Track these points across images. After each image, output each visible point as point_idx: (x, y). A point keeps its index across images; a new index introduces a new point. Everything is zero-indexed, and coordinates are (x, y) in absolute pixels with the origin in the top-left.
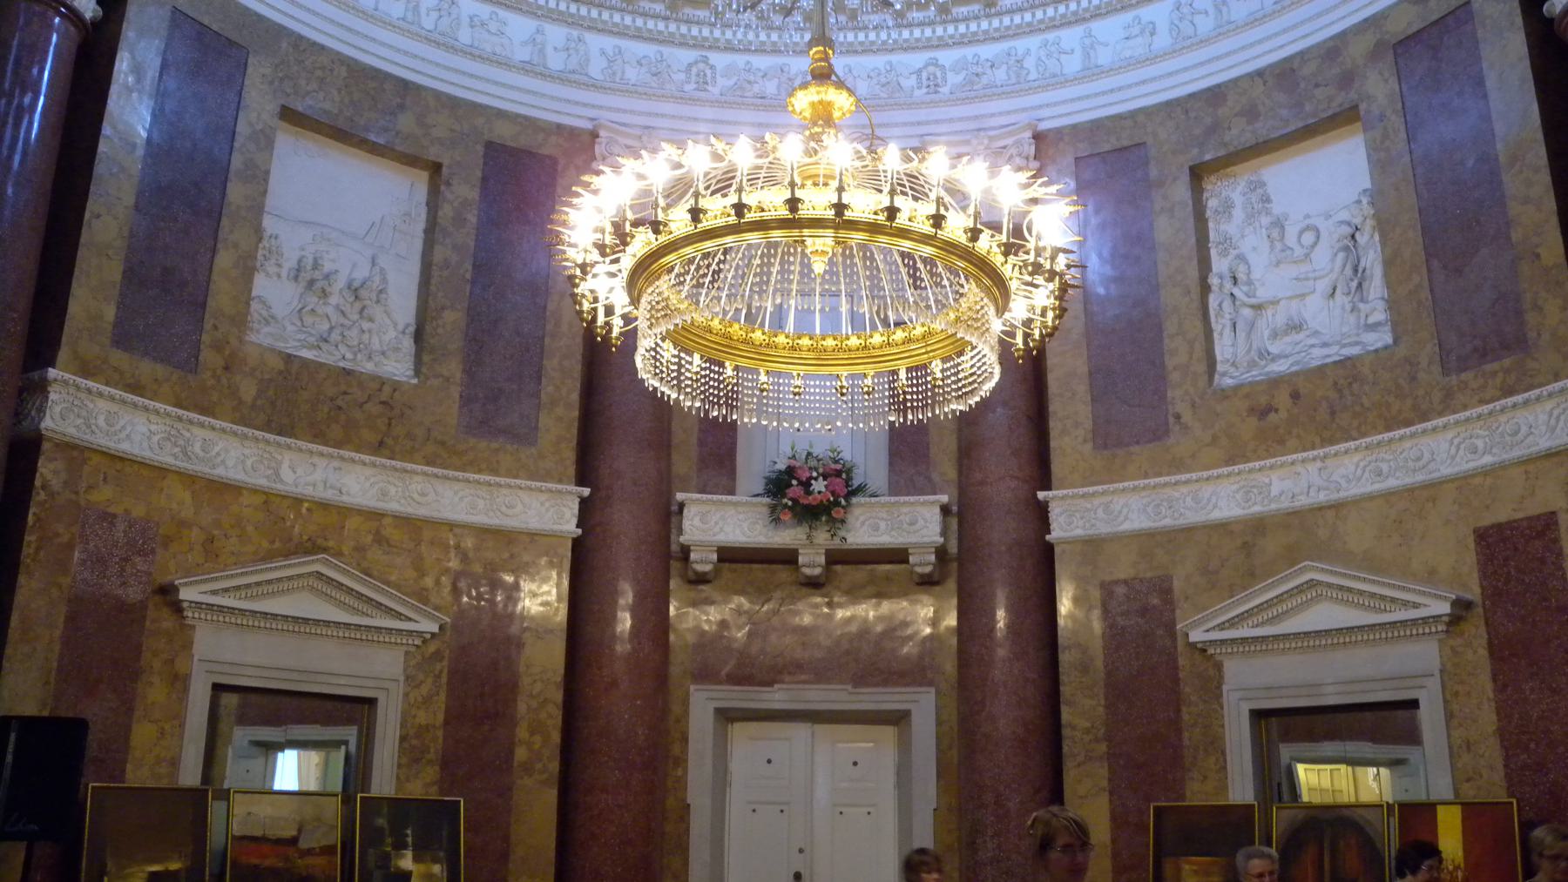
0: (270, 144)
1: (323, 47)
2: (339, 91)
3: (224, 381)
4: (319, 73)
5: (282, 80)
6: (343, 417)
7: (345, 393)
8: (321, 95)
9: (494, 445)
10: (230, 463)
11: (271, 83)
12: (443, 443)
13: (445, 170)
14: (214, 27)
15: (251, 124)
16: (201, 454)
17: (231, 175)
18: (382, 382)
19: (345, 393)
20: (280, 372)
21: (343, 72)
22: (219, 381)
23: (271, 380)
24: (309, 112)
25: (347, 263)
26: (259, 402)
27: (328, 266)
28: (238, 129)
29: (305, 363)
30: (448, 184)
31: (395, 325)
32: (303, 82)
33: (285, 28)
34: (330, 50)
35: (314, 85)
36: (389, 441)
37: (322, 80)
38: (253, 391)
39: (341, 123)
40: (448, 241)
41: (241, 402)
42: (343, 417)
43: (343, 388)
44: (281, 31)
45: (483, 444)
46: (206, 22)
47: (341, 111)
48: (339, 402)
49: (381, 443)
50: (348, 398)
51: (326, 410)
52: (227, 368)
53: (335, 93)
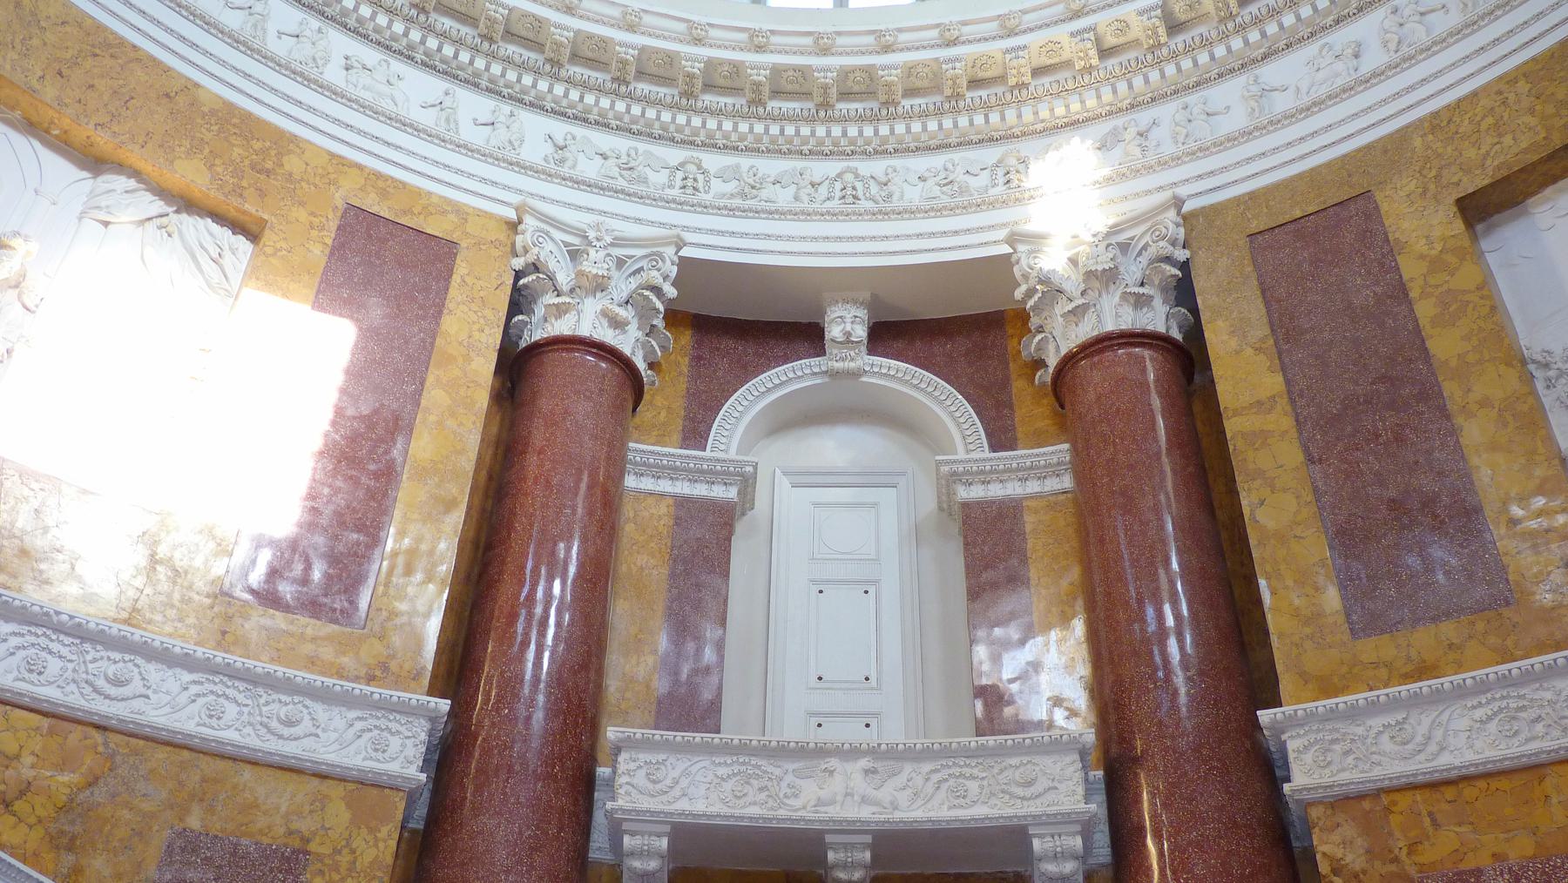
1: (1475, 94)
2: (1532, 111)
5: (1438, 177)
8: (1508, 140)
14: (1311, 209)
15: (1422, 257)
21: (1523, 86)
24: (1504, 172)
28: (1406, 277)
32: (1471, 153)
33: (1407, 127)
34: (1485, 88)
44: (1402, 135)
46: (1298, 214)
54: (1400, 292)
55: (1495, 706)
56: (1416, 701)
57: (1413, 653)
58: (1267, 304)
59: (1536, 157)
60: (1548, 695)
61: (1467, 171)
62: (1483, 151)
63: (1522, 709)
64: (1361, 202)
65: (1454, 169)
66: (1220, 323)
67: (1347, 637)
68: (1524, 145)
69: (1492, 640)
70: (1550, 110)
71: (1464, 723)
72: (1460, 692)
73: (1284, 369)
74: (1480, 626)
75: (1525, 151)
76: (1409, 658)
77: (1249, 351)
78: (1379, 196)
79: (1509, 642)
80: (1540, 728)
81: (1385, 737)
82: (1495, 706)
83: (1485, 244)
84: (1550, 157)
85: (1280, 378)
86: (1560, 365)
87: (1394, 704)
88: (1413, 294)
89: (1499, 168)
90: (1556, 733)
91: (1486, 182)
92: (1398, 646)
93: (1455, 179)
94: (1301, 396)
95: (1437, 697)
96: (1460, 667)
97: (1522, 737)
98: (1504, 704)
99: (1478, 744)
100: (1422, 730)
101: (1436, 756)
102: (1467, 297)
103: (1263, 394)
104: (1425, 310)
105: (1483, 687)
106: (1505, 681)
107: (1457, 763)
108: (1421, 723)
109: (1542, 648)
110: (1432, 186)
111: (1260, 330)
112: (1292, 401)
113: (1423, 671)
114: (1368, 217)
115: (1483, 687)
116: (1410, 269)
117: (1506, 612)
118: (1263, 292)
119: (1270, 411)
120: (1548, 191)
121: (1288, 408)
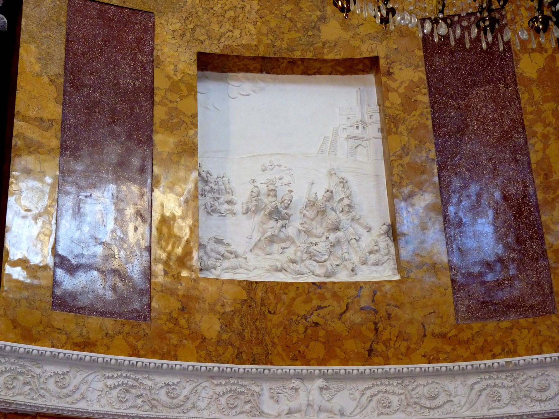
0: (193, 91)
3: (182, 322)
4: (231, 14)
5: (193, 30)
6: (322, 333)
7: (320, 308)
8: (237, 33)
9: (505, 324)
10: (202, 405)
11: (183, 35)
12: (443, 336)
13: (382, 62)
15: (168, 77)
16: (168, 401)
17: (156, 127)
18: (358, 286)
19: (320, 308)
20: (244, 302)
22: (176, 323)
23: (234, 312)
24: (227, 52)
25: (305, 183)
26: (225, 336)
27: (282, 192)
28: (156, 84)
29: (269, 287)
30: (389, 74)
31: (369, 230)
32: (216, 27)
35: (227, 26)
36: (380, 348)
37: (234, 19)
38: (217, 326)
39: (261, 52)
40: (402, 128)
41: (204, 339)
42: (322, 333)
43: (316, 303)
45: (491, 325)
47: (260, 41)
48: (314, 318)
49: (370, 351)
50: (322, 312)
51: (301, 329)
52: (183, 309)
53: (251, 27)
54: (150, 92)
55: (121, 380)
56: (80, 364)
57: (85, 331)
58: (67, 50)
59: (247, 54)
60: (150, 383)
61: (210, 38)
62: (222, 30)
63: (133, 387)
64: (145, 17)
65: (203, 31)
66: (33, 47)
67: (48, 306)
68: (244, 42)
69: (131, 339)
70: (264, 30)
71: (98, 385)
72: (106, 366)
73: (64, 103)
74: (127, 328)
75: (244, 46)
76: (81, 335)
77: (46, 79)
78: (157, 21)
79: (139, 344)
80: (139, 401)
81: (52, 381)
82: (121, 380)
83: (202, 87)
84: (254, 59)
85: (59, 109)
86: (212, 185)
87: (67, 361)
88: (157, 99)
89: (227, 47)
90: (147, 407)
91: (218, 51)
92: (77, 324)
93: (202, 38)
94: (69, 130)
95: (92, 366)
96: (107, 350)
97: (129, 404)
98: (126, 381)
99: (104, 401)
100: (75, 382)
101: (78, 401)
102: (184, 118)
103: (46, 115)
104: (160, 113)
105: (119, 367)
106: (133, 368)
107: (90, 409)
108: (76, 378)
109: (154, 354)
110: (188, 34)
111: (57, 68)
112: (62, 130)
113: (86, 345)
114: (146, 31)
115: (119, 367)
116: (160, 82)
117: (143, 325)
118: (67, 41)
119: (47, 129)
120: (241, 75)
121: (59, 134)
